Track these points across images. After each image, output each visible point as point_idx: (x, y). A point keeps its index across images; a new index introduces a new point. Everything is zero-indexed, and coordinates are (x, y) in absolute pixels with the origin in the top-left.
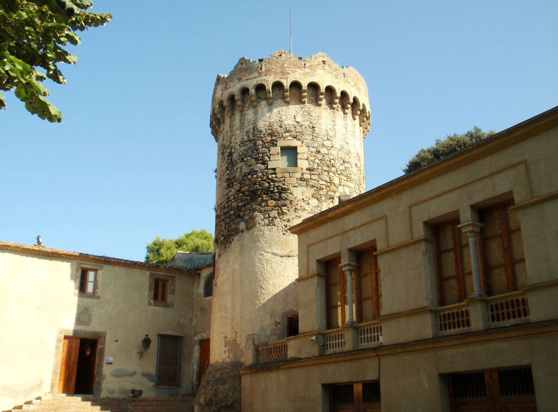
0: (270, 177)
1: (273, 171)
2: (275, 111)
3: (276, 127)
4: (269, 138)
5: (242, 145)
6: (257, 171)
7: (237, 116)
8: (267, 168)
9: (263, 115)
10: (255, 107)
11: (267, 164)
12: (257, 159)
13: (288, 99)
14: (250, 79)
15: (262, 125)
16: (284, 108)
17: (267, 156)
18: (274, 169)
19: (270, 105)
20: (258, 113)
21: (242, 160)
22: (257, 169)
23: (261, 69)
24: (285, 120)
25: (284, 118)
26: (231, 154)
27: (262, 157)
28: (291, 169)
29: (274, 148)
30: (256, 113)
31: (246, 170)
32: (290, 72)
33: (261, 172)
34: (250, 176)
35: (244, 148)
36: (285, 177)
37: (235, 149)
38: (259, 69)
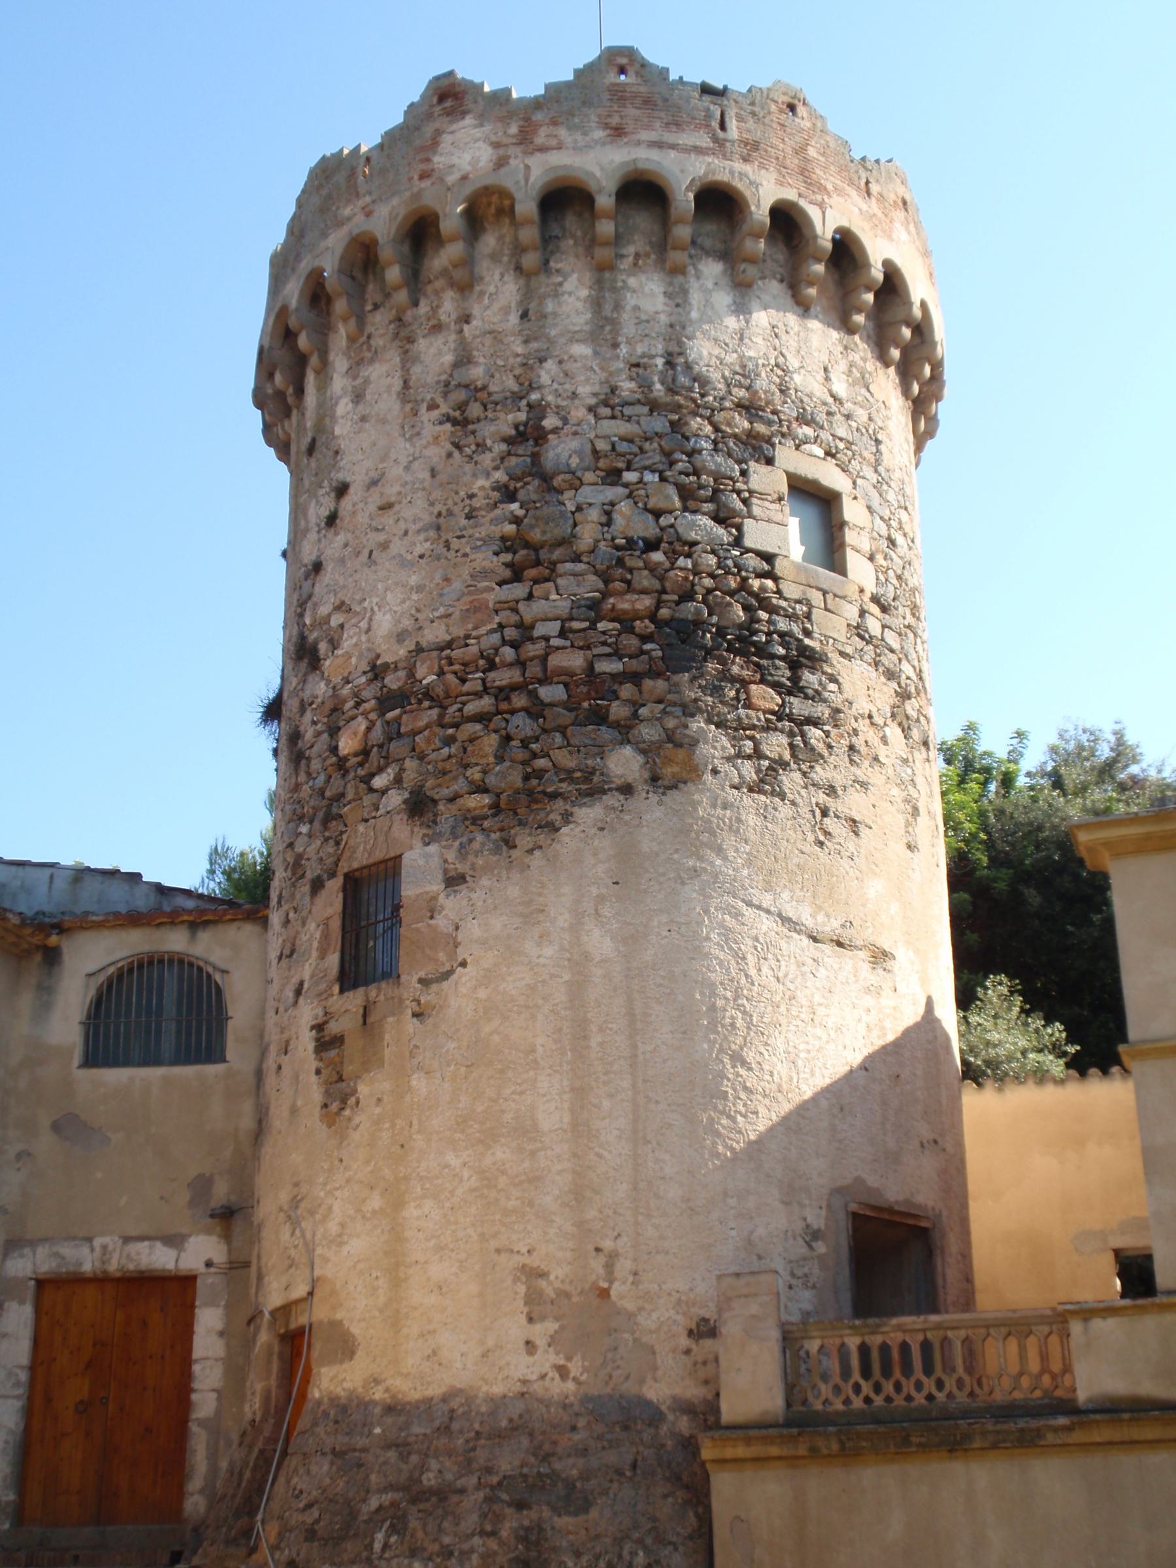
0: (755, 584)
1: (766, 567)
2: (761, 318)
3: (764, 383)
4: (742, 424)
5: (606, 411)
6: (694, 544)
8: (738, 542)
10: (678, 271)
11: (739, 528)
12: (686, 494)
13: (812, 291)
14: (673, 147)
15: (707, 352)
16: (792, 319)
17: (739, 493)
18: (769, 558)
19: (742, 290)
20: (686, 300)
21: (613, 477)
22: (693, 536)
23: (723, 127)
24: (797, 371)
25: (793, 362)
26: (530, 434)
27: (716, 491)
28: (826, 576)
29: (763, 469)
30: (678, 298)
31: (631, 522)
32: (830, 187)
33: (713, 552)
34: (657, 556)
35: (620, 428)
36: (810, 606)
37: (565, 421)
38: (715, 124)
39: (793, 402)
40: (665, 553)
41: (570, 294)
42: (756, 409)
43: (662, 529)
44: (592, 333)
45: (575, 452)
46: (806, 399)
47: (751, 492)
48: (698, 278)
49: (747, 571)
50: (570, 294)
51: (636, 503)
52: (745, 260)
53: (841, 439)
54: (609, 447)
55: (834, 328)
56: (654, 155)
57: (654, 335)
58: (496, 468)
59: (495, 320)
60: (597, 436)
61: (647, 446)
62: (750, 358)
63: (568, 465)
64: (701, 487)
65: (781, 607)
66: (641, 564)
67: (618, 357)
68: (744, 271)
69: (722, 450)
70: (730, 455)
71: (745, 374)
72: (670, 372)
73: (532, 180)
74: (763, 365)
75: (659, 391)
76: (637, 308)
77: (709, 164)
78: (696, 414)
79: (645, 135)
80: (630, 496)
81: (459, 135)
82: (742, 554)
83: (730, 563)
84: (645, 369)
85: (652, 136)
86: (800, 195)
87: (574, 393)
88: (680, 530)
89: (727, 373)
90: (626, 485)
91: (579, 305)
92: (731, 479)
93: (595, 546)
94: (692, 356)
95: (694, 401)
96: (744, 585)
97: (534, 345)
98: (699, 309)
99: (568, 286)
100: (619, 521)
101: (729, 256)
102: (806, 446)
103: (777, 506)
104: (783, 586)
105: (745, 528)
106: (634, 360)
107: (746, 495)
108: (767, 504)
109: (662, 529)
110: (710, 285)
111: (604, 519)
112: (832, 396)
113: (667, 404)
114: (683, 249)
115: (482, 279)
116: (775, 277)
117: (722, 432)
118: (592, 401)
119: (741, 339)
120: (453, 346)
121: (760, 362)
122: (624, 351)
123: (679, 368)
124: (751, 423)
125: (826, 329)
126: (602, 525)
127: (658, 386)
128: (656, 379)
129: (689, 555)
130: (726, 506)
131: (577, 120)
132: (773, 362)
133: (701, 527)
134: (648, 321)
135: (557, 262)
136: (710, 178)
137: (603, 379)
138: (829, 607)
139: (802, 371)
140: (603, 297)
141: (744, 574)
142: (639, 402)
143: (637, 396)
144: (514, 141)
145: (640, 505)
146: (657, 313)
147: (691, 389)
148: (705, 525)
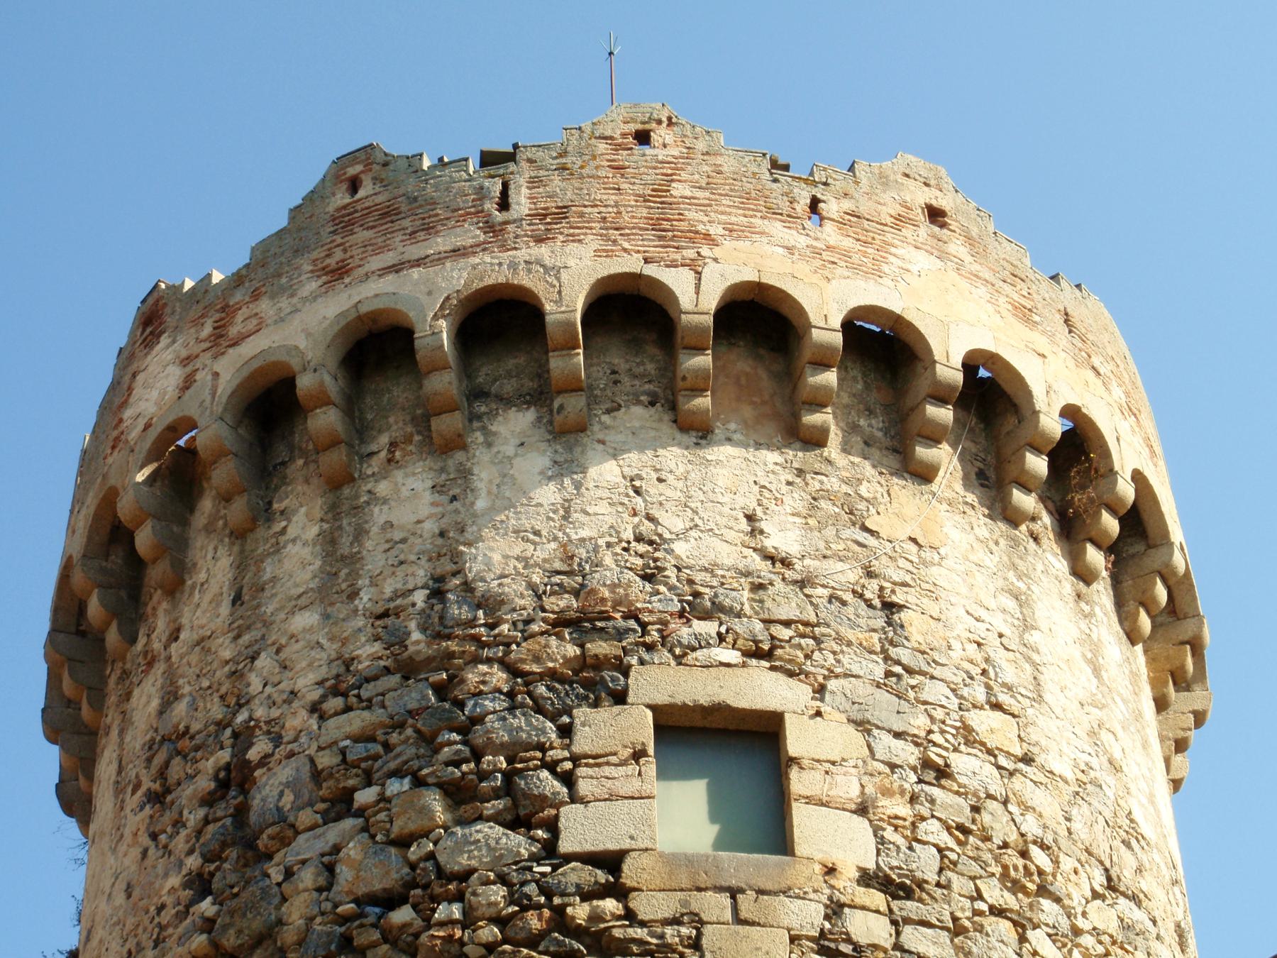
0: (580, 912)
1: (602, 876)
2: (605, 473)
3: (613, 575)
4: (564, 649)
5: (336, 703)
6: (465, 875)
7: (299, 518)
8: (549, 849)
9: (510, 494)
10: (456, 444)
11: (553, 827)
12: (461, 796)
13: (704, 402)
14: (418, 263)
15: (503, 558)
16: (674, 457)
17: (552, 767)
18: (611, 861)
19: (568, 437)
20: (468, 488)
21: (341, 806)
22: (464, 861)
23: (504, 205)
24: (681, 536)
25: (671, 522)
26: (236, 779)
27: (509, 776)
28: (747, 866)
29: (607, 713)
30: (454, 488)
31: (365, 868)
32: (716, 230)
33: (503, 880)
34: (403, 915)
35: (358, 720)
36: (699, 922)
37: (277, 740)
38: (490, 206)
39: (671, 588)
40: (414, 907)
41: (294, 541)
42: (591, 621)
43: (413, 867)
44: (320, 589)
45: (287, 785)
46: (699, 577)
47: (575, 759)
48: (489, 445)
49: (563, 894)
50: (294, 541)
51: (373, 837)
52: (559, 392)
53: (787, 624)
54: (337, 759)
55: (769, 447)
56: (386, 284)
57: (413, 558)
58: (191, 852)
59: (204, 621)
60: (320, 749)
61: (394, 738)
62: (583, 540)
63: (279, 809)
64: (483, 776)
65: (634, 940)
66: (376, 935)
67: (356, 611)
68: (561, 407)
69: (523, 705)
70: (539, 710)
71: (573, 570)
72: (438, 607)
73: (219, 391)
74: (609, 545)
75: (417, 642)
76: (389, 525)
77: (474, 267)
78: (476, 660)
79: (376, 263)
80: (365, 829)
81: (150, 369)
82: (554, 870)
83: (531, 889)
84: (397, 615)
85: (389, 258)
86: (646, 261)
87: (292, 692)
88: (442, 859)
89: (536, 579)
90: (360, 813)
91: (306, 552)
92: (542, 748)
93: (308, 928)
94: (473, 568)
95: (476, 639)
96: (560, 920)
97: (246, 638)
98: (489, 493)
99: (292, 532)
100: (344, 873)
101: (541, 394)
102: (691, 656)
103: (632, 768)
104: (640, 904)
105: (562, 823)
106: (379, 609)
107: (568, 765)
108: (607, 770)
109: (413, 867)
110: (510, 450)
111: (322, 881)
112: (771, 558)
113: (429, 660)
114: (452, 409)
115: (195, 565)
116: (639, 402)
117: (522, 674)
118: (316, 695)
119: (566, 517)
120: (159, 683)
121: (601, 542)
122: (365, 599)
123: (450, 596)
124: (582, 646)
125: (751, 453)
126: (319, 890)
127: (416, 635)
128: (412, 625)
129: (459, 897)
130: (527, 795)
131: (284, 280)
132: (628, 535)
133: (491, 839)
134: (404, 541)
135: (281, 501)
136: (477, 285)
137: (334, 655)
138: (744, 914)
139: (693, 533)
140: (340, 528)
141: (557, 901)
142: (387, 671)
143: (382, 663)
144: (207, 345)
145: (379, 838)
146: (419, 522)
147: (472, 623)
148: (487, 837)
